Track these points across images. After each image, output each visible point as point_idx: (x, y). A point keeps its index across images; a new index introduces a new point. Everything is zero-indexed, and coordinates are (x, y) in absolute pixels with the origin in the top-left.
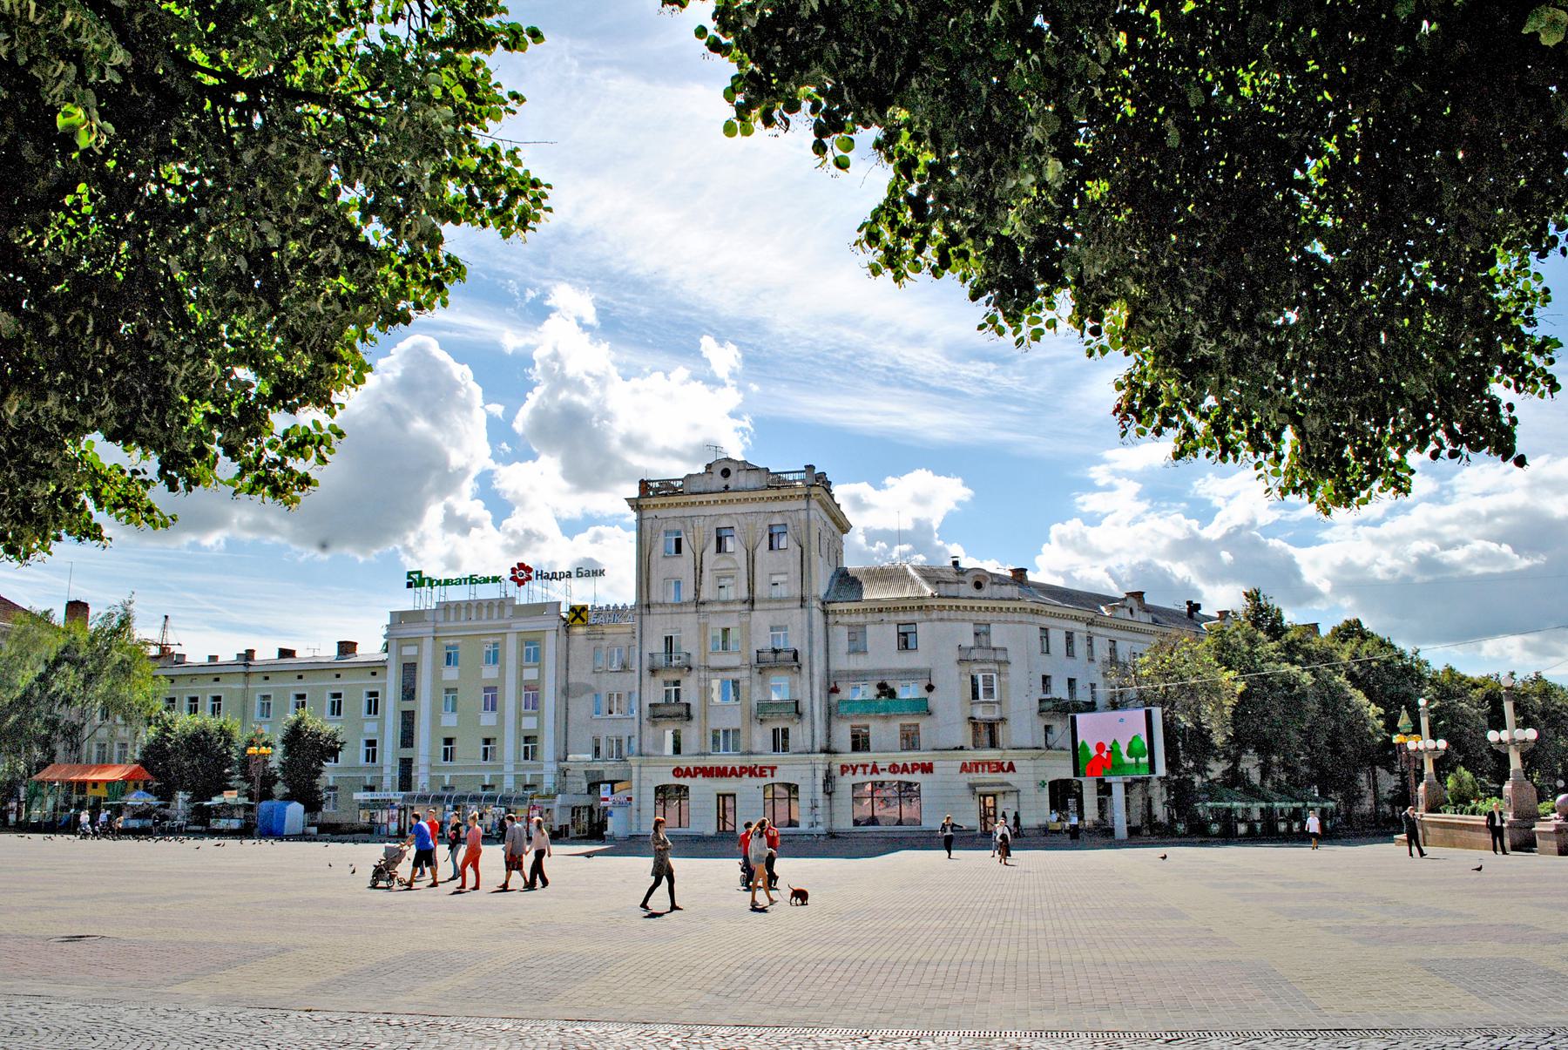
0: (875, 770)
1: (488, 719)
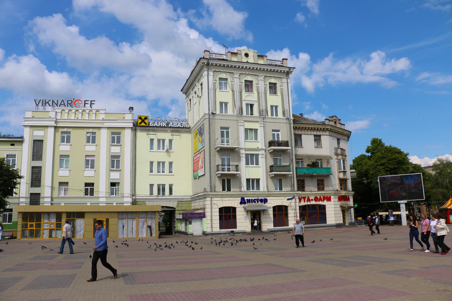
0: (309, 200)
1: (89, 174)
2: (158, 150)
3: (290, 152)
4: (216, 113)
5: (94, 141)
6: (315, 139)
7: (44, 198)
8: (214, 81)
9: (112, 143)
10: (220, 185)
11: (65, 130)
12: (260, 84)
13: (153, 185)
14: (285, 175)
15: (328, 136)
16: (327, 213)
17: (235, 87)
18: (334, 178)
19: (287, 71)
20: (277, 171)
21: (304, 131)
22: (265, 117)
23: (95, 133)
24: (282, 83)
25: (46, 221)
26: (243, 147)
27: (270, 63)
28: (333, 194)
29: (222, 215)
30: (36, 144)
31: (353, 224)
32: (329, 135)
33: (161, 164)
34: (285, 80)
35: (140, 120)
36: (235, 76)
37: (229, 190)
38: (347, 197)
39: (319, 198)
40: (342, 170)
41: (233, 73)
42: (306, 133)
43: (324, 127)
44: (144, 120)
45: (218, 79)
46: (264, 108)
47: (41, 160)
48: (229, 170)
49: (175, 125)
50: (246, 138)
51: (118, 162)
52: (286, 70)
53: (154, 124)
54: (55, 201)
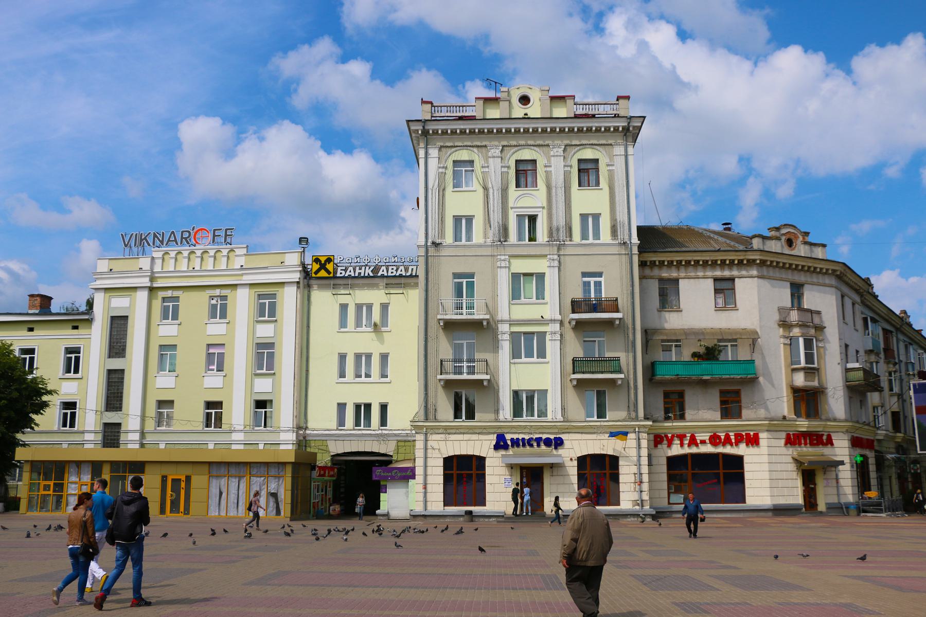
0: (693, 442)
1: (214, 381)
2: (357, 327)
3: (629, 322)
4: (441, 243)
5: (223, 315)
6: (718, 288)
7: (127, 432)
8: (441, 170)
9: (260, 317)
10: (449, 405)
11: (169, 293)
12: (553, 166)
13: (345, 404)
14: (613, 381)
15: (756, 279)
16: (747, 476)
17: (489, 180)
18: (773, 385)
19: (624, 128)
20: (583, 373)
21: (686, 270)
22: (563, 243)
23: (224, 298)
24: (611, 157)
25: (74, 478)
26: (506, 317)
27: (584, 112)
28: (766, 428)
29: (472, 474)
30: (116, 325)
31: (842, 508)
32: (759, 277)
33: (363, 359)
34: (619, 150)
35: (317, 264)
36: (490, 154)
37: (471, 416)
38: (823, 435)
39: (723, 437)
40: (803, 364)
41: (485, 146)
42: (692, 274)
43: (741, 258)
44: (325, 264)
45: (450, 164)
46: (562, 222)
47: (124, 357)
48: (471, 371)
49: (392, 271)
50: (515, 294)
51: (271, 356)
52: (621, 124)
53: (346, 273)
54: (149, 438)
